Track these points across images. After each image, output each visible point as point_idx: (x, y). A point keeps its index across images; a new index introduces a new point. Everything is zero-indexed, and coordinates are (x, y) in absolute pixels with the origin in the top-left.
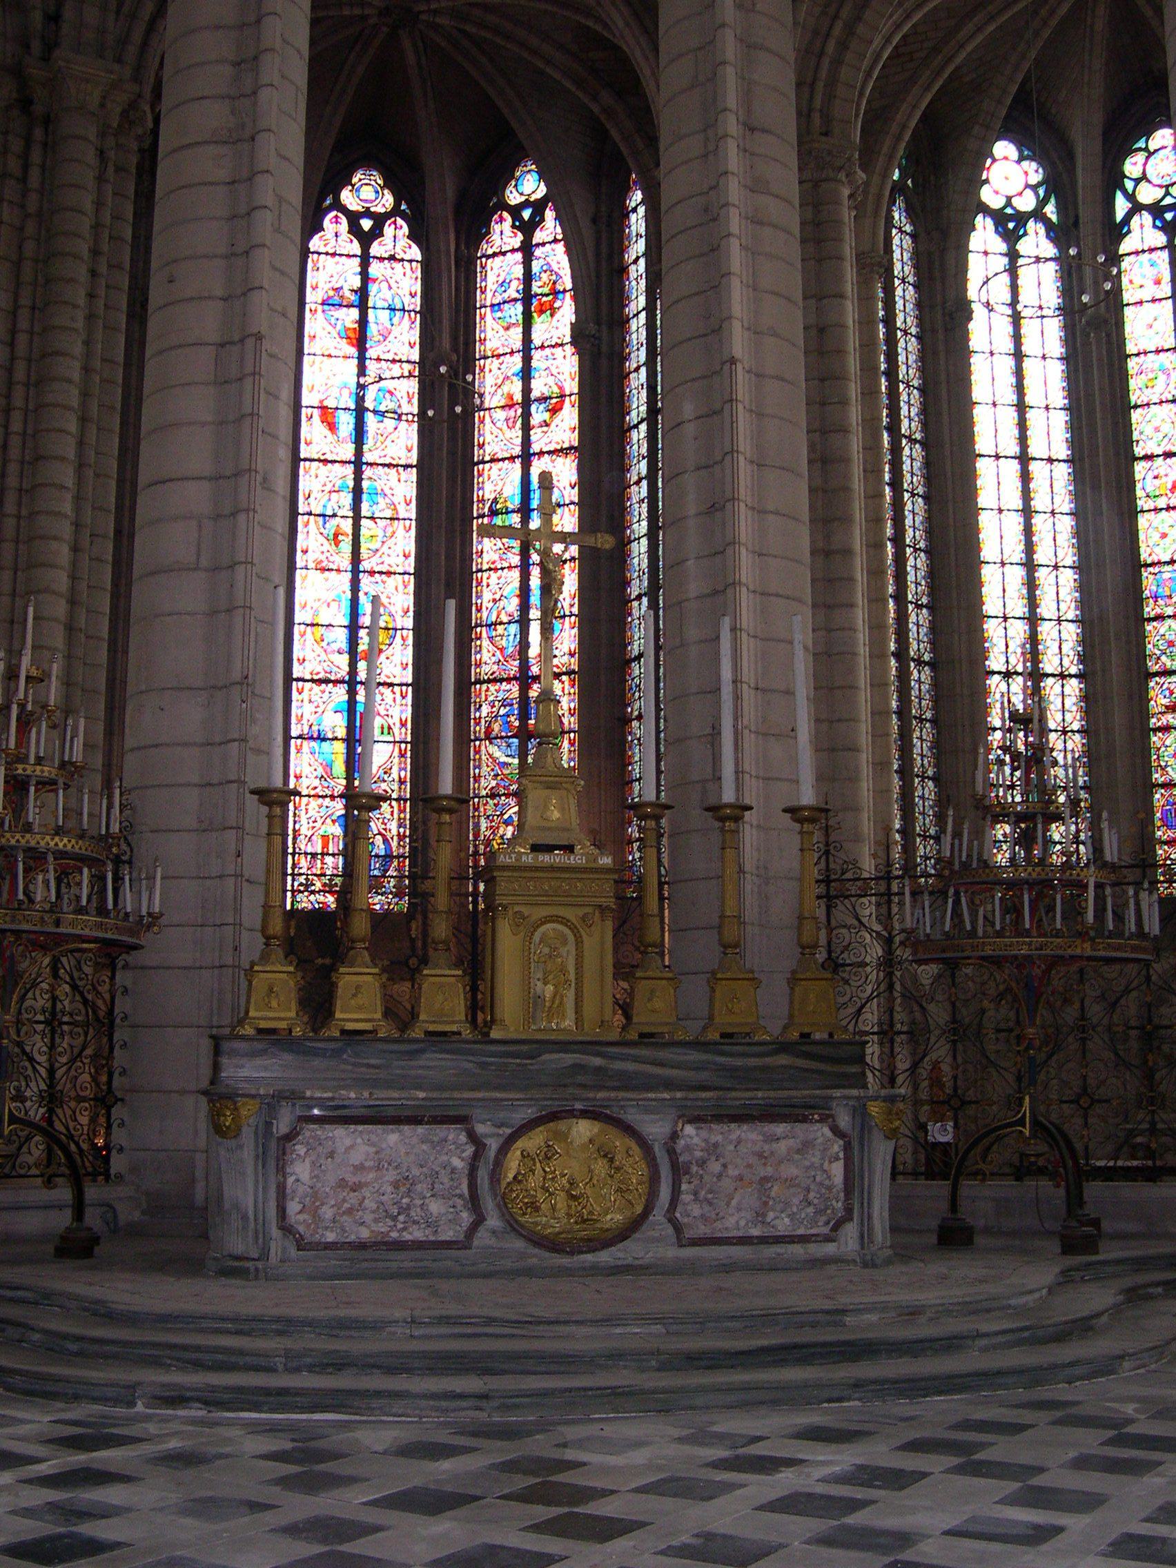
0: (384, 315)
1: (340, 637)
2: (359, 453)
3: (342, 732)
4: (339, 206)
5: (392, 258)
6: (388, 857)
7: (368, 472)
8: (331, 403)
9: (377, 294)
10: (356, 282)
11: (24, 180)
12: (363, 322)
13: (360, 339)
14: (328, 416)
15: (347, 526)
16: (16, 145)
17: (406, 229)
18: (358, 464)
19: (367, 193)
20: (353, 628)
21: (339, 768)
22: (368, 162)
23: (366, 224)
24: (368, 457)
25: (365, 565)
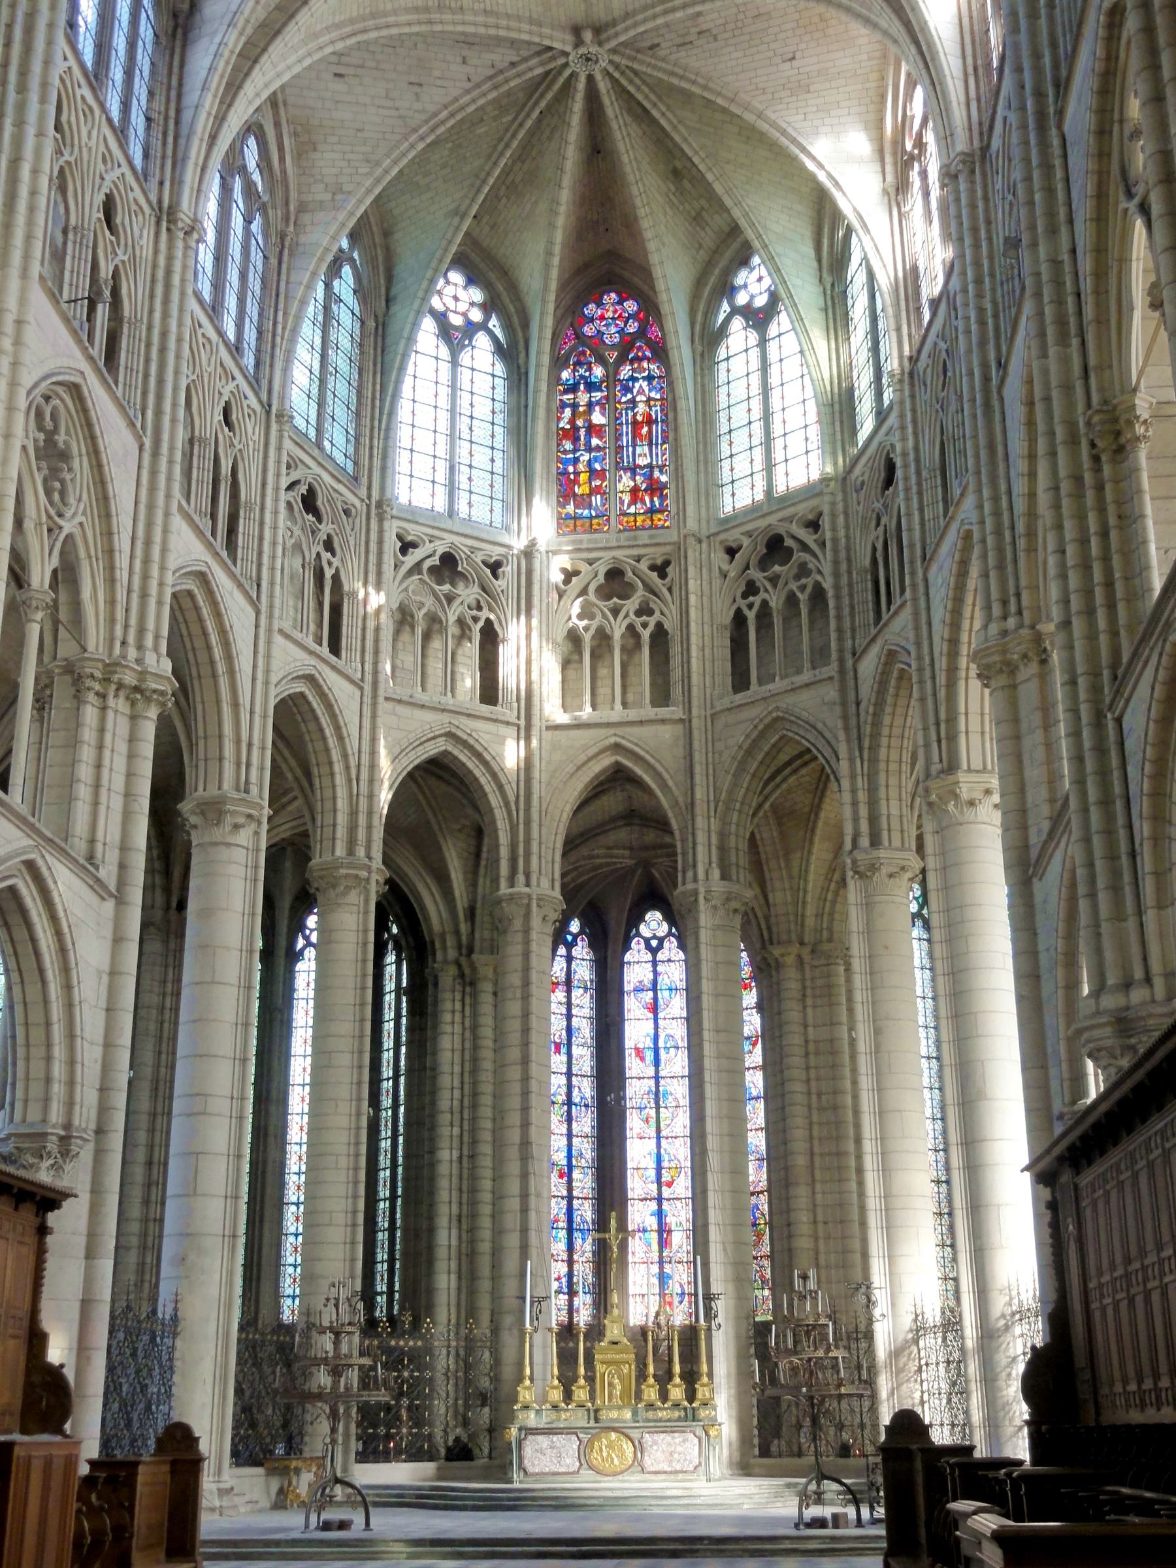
0: (666, 994)
1: (652, 1174)
2: (657, 1071)
3: (655, 1227)
4: (638, 934)
5: (669, 960)
6: (683, 1294)
7: (662, 1082)
8: (641, 1046)
9: (663, 982)
10: (651, 976)
11: (463, 1011)
12: (655, 999)
13: (654, 1008)
14: (639, 1053)
15: (653, 1113)
16: (458, 996)
17: (675, 943)
18: (657, 1078)
19: (654, 925)
20: (659, 1169)
21: (655, 1246)
22: (654, 907)
23: (654, 943)
24: (662, 1073)
25: (663, 1134)
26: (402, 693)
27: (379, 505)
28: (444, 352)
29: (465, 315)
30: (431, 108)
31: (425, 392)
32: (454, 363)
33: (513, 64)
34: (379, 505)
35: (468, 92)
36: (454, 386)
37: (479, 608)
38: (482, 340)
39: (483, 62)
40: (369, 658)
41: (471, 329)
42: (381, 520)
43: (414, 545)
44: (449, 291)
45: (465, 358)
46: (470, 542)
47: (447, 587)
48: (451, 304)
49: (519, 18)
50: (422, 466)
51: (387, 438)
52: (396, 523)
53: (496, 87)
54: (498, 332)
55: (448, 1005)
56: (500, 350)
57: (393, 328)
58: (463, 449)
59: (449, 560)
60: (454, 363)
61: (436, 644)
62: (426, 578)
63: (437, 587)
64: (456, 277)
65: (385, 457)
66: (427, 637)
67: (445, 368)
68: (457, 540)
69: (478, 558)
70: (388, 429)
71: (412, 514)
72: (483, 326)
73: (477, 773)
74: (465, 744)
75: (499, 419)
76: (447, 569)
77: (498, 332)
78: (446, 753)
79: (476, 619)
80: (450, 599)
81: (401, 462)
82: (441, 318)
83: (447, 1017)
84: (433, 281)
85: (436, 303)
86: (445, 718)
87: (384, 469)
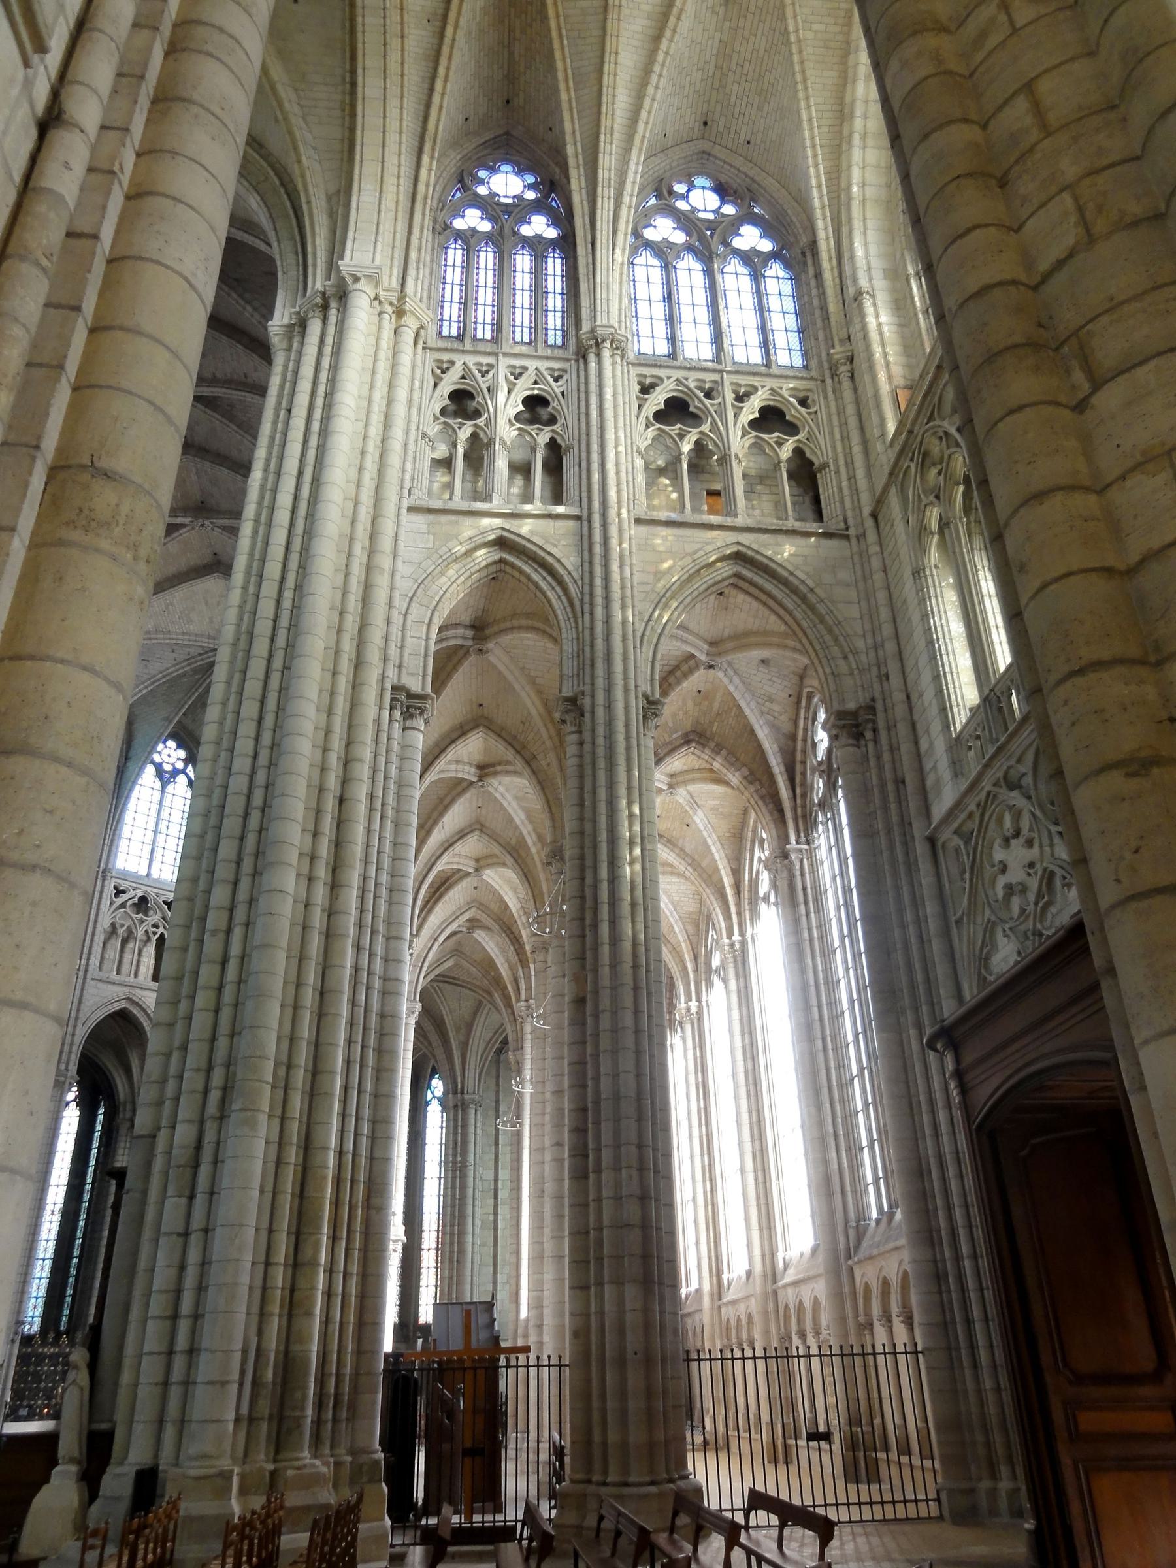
26: (103, 975)
27: (104, 871)
28: (158, 785)
29: (173, 765)
30: (155, 672)
31: (143, 807)
32: (163, 792)
33: (200, 654)
34: (104, 871)
35: (174, 665)
36: (160, 804)
37: (158, 927)
38: (181, 778)
39: (181, 655)
40: (84, 956)
41: (175, 773)
42: (104, 880)
43: (124, 892)
44: (166, 751)
45: (170, 788)
46: (157, 891)
47: (140, 915)
48: (166, 759)
49: (202, 636)
50: (135, 847)
51: (114, 835)
52: (114, 880)
53: (190, 665)
54: (192, 776)
55: (122, 1145)
56: (191, 783)
57: (127, 774)
58: (161, 838)
59: (143, 900)
60: (163, 792)
61: (130, 945)
62: (128, 910)
63: (134, 916)
64: (171, 744)
65: (111, 846)
66: (125, 941)
67: (157, 795)
68: (149, 889)
69: (160, 900)
70: (115, 830)
71: (125, 875)
72: (183, 771)
73: (142, 1020)
74: (137, 1004)
75: (185, 823)
76: (142, 904)
77: (192, 776)
78: (125, 1009)
79: (155, 934)
80: (142, 921)
81: (123, 845)
82: (159, 768)
83: (120, 1152)
84: (156, 744)
85: (157, 758)
86: (126, 990)
87: (110, 851)
